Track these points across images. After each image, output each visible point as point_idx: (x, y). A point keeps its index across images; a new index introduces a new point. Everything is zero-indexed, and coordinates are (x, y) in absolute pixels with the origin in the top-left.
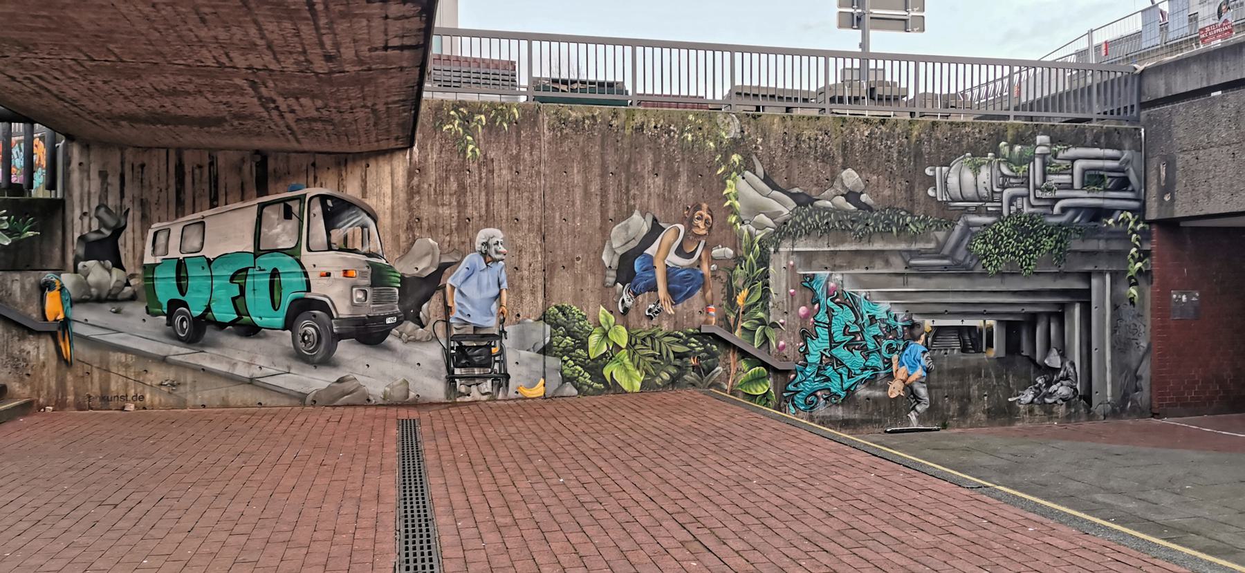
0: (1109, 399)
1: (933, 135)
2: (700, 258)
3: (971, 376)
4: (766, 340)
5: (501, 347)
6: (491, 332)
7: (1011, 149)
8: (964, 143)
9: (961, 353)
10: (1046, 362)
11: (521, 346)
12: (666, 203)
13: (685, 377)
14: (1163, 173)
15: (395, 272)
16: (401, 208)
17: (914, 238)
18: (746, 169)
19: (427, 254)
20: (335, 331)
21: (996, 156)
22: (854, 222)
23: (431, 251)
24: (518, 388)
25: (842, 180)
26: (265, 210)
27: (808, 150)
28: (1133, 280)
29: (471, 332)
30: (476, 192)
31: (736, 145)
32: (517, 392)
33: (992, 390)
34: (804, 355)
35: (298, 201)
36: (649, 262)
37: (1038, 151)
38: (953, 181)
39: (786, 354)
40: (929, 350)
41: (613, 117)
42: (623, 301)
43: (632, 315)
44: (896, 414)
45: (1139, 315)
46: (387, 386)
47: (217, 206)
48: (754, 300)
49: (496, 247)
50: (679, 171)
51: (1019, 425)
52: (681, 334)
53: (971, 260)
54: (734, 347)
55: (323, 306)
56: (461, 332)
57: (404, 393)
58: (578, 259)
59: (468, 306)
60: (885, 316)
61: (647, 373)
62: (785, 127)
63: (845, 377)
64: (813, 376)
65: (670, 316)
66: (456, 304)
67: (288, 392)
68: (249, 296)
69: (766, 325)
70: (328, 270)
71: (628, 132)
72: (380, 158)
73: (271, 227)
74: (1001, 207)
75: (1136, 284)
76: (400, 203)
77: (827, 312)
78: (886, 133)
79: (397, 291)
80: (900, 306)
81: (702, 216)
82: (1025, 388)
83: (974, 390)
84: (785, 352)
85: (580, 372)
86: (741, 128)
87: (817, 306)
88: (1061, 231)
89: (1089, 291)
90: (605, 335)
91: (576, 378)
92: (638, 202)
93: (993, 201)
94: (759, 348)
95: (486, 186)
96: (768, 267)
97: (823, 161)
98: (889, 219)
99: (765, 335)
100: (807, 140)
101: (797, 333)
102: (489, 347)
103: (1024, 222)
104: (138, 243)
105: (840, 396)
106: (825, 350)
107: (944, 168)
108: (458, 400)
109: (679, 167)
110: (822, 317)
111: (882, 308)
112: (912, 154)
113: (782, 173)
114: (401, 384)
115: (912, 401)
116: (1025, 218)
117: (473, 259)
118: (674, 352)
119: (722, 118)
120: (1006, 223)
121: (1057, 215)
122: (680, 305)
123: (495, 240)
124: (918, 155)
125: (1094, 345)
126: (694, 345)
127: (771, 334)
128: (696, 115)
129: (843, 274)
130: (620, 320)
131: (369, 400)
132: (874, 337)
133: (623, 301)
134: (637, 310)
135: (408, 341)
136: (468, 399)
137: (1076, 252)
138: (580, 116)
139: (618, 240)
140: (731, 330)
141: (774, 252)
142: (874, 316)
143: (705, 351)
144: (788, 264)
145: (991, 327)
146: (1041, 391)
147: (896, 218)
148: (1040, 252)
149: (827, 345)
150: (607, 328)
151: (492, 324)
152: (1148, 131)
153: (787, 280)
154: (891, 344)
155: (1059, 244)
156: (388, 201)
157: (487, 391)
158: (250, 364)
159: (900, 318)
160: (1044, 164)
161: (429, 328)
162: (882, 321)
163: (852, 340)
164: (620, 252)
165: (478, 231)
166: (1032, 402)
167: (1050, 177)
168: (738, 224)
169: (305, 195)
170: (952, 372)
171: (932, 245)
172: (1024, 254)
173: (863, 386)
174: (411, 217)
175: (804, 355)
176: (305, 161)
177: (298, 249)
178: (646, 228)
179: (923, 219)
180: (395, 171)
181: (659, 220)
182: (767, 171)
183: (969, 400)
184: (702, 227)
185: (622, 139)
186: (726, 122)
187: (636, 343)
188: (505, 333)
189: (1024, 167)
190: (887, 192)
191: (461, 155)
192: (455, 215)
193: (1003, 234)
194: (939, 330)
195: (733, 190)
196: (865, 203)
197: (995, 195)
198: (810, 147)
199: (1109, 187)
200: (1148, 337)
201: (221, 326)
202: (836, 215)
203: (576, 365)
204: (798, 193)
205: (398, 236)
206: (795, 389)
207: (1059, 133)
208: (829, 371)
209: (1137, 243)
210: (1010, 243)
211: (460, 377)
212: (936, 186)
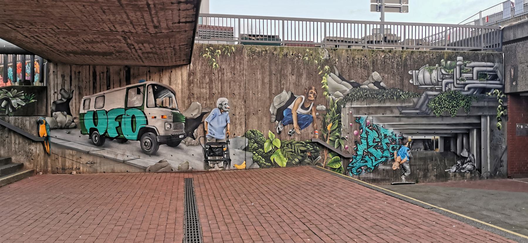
0: (489, 170)
1: (412, 57)
2: (311, 110)
3: (428, 160)
4: (340, 145)
5: (227, 148)
6: (223, 142)
7: (446, 63)
8: (426, 60)
9: (424, 151)
10: (461, 154)
11: (236, 147)
12: (297, 87)
13: (305, 160)
14: (512, 73)
15: (183, 116)
16: (185, 89)
17: (404, 101)
18: (331, 72)
19: (196, 109)
20: (158, 141)
21: (440, 66)
22: (377, 94)
23: (198, 107)
24: (234, 165)
25: (372, 76)
26: (129, 91)
27: (358, 64)
28: (499, 119)
29: (215, 141)
30: (217, 82)
31: (327, 62)
32: (234, 167)
33: (438, 167)
34: (356, 151)
35: (143, 87)
36: (290, 112)
37: (458, 63)
38: (421, 76)
39: (348, 151)
40: (410, 149)
41: (274, 50)
42: (279, 128)
43: (283, 134)
44: (396, 177)
45: (502, 134)
46: (180, 164)
47: (110, 89)
48: (335, 128)
49: (225, 105)
50: (302, 73)
51: (450, 181)
52: (303, 142)
53: (429, 110)
54: (326, 148)
55: (153, 131)
56: (210, 141)
57: (187, 167)
58: (260, 110)
59: (213, 130)
60: (391, 135)
61: (289, 159)
62: (348, 54)
63: (374, 161)
64: (360, 160)
65: (298, 135)
66: (208, 130)
67: (139, 166)
68: (123, 126)
69: (340, 138)
70: (155, 115)
71: (281, 57)
72: (177, 69)
73: (132, 98)
74: (442, 88)
75: (501, 120)
76: (185, 87)
77: (366, 133)
78: (391, 56)
79: (184, 124)
80: (397, 130)
81: (312, 92)
82: (453, 166)
83: (430, 167)
84: (348, 150)
85: (261, 158)
86: (329, 54)
87: (361, 130)
88: (468, 98)
89: (480, 124)
90: (271, 143)
91: (259, 161)
92: (285, 86)
93: (438, 85)
94: (337, 148)
95: (221, 80)
96: (341, 114)
97: (364, 68)
98: (393, 93)
99: (339, 143)
100: (357, 60)
101: (353, 142)
102: (222, 148)
103: (452, 94)
104: (77, 104)
105: (371, 169)
106: (365, 149)
107: (417, 71)
108: (209, 170)
109: (302, 71)
110: (364, 135)
111: (390, 131)
112: (403, 65)
113: (346, 73)
114: (186, 163)
115: (403, 171)
116: (452, 92)
117: (215, 111)
118: (300, 150)
119: (321, 50)
120: (444, 95)
121: (466, 91)
122: (303, 130)
123: (224, 103)
124: (405, 65)
125: (482, 147)
126: (309, 147)
127: (342, 142)
128: (310, 49)
129: (373, 117)
130: (277, 136)
131: (172, 170)
132: (386, 143)
133: (279, 128)
134: (285, 132)
135: (189, 145)
136: (213, 169)
137: (474, 107)
138: (260, 50)
139: (277, 102)
140: (325, 140)
141: (343, 107)
142: (386, 135)
143: (314, 149)
144: (349, 112)
145: (438, 139)
146: (459, 167)
147: (396, 93)
148: (459, 107)
149: (366, 147)
150: (272, 140)
151: (223, 138)
152: (506, 55)
153: (349, 119)
154: (394, 147)
155: (467, 104)
156: (180, 87)
157: (221, 166)
158: (123, 155)
159: (397, 135)
160: (461, 69)
161: (197, 140)
162: (390, 136)
163: (377, 145)
164: (277, 107)
165: (217, 99)
166: (455, 172)
167: (463, 75)
168: (328, 95)
169: (146, 84)
170: (421, 159)
171: (411, 104)
172: (452, 108)
173: (381, 165)
174: (190, 93)
175: (356, 151)
176: (145, 70)
177: (143, 107)
178: (288, 97)
179: (408, 93)
180: (183, 74)
181: (293, 93)
182: (340, 73)
183: (428, 171)
184: (312, 97)
185: (278, 60)
186: (323, 52)
187: (284, 146)
188: (229, 142)
189: (452, 70)
190: (392, 82)
191: (211, 67)
192: (208, 92)
193: (443, 99)
194: (414, 141)
195: (326, 81)
196: (382, 87)
197: (439, 82)
198: (358, 63)
199: (489, 79)
200: (506, 144)
201: (111, 139)
202: (370, 91)
203: (259, 155)
204: (353, 82)
205: (184, 101)
206: (352, 166)
207: (467, 56)
208: (367, 158)
209: (501, 103)
210: (446, 103)
211: (210, 160)
212: (413, 79)
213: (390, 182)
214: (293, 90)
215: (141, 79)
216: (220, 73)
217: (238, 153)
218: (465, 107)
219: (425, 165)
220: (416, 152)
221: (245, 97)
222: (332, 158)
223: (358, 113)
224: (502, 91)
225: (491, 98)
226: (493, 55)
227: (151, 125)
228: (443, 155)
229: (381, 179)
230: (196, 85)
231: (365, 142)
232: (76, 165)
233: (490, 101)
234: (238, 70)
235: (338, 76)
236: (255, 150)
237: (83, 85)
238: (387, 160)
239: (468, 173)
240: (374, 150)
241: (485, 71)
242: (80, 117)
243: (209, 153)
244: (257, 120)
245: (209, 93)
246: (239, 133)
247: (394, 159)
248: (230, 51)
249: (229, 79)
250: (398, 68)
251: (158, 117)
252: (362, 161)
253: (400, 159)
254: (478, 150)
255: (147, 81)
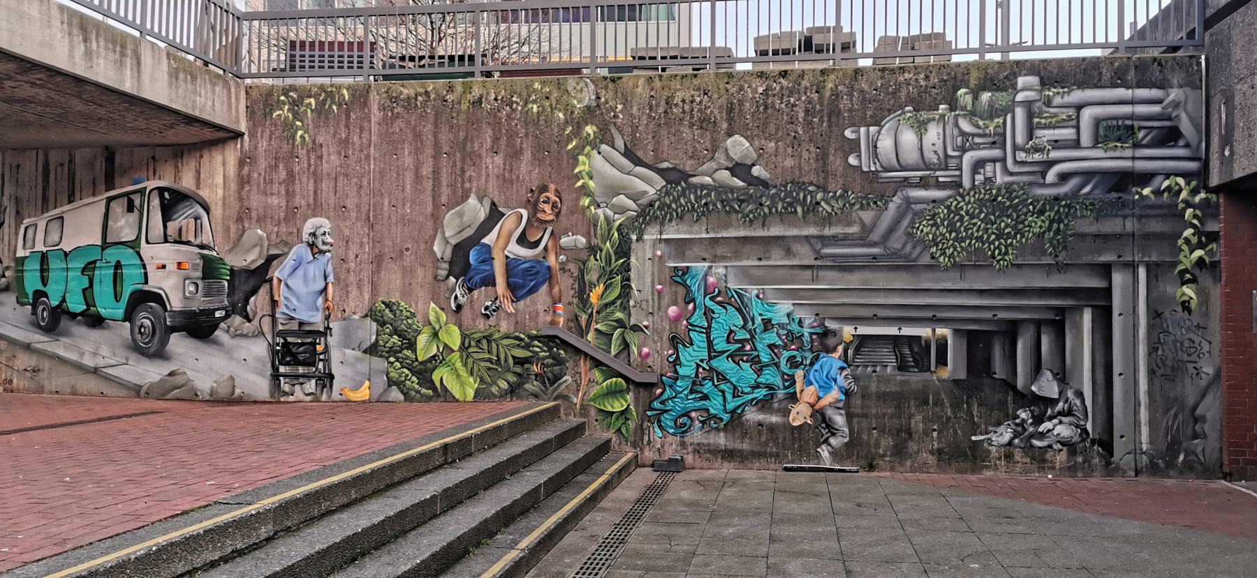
0: (1144, 447)
1: (856, 87)
2: (546, 248)
3: (912, 403)
4: (626, 346)
5: (326, 344)
6: (316, 329)
7: (976, 98)
8: (903, 94)
9: (897, 372)
10: (1033, 388)
11: (346, 345)
12: (506, 184)
13: (527, 386)
14: (1224, 116)
15: (225, 264)
16: (232, 199)
17: (828, 220)
18: (602, 142)
19: (256, 246)
20: (168, 323)
21: (952, 109)
22: (742, 201)
23: (259, 242)
24: (342, 390)
25: (726, 150)
26: (111, 204)
27: (682, 115)
28: (1188, 276)
29: (296, 328)
30: (304, 179)
31: (590, 113)
32: (341, 394)
33: (945, 424)
34: (675, 366)
35: (139, 195)
36: (486, 253)
37: (1020, 97)
38: (885, 143)
39: (651, 364)
40: (849, 366)
41: (448, 91)
42: (456, 297)
43: (466, 312)
44: (800, 446)
45: (1198, 327)
46: (215, 382)
47: (74, 201)
48: (611, 298)
49: (323, 237)
50: (521, 148)
51: (988, 474)
52: (523, 336)
53: (914, 248)
54: (586, 355)
55: (157, 298)
56: (286, 327)
57: (230, 389)
58: (407, 249)
59: (294, 300)
60: (785, 320)
61: (482, 380)
62: (652, 89)
63: (729, 396)
64: (686, 392)
65: (509, 315)
66: (282, 297)
67: (126, 383)
68: (96, 287)
69: (626, 328)
70: (163, 262)
71: (464, 107)
72: (214, 148)
73: (116, 221)
74: (961, 176)
75: (1194, 280)
76: (232, 193)
77: (705, 314)
78: (787, 88)
79: (226, 284)
80: (807, 307)
81: (548, 198)
82: (1000, 424)
83: (917, 423)
84: (649, 361)
85: (407, 375)
86: (597, 94)
87: (691, 306)
88: (1062, 208)
89: (1108, 292)
90: (435, 335)
91: (403, 382)
92: (475, 184)
93: (946, 169)
94: (616, 356)
95: (315, 173)
96: (629, 259)
97: (702, 128)
98: (792, 197)
99: (624, 339)
100: (681, 104)
101: (665, 338)
102: (314, 344)
103: (997, 196)
104: (13, 237)
105: (721, 419)
106: (702, 361)
107: (872, 129)
108: (282, 399)
109: (522, 143)
110: (699, 319)
111: (782, 309)
112: (825, 112)
113: (647, 144)
114: (227, 380)
115: (824, 432)
116: (999, 190)
117: (300, 250)
118: (514, 357)
119: (574, 84)
120: (967, 198)
121: (1052, 185)
122: (522, 302)
123: (322, 231)
124: (834, 113)
125: (1117, 368)
126: (537, 349)
127: (632, 338)
128: (543, 83)
129: (726, 267)
130: (452, 318)
131: (196, 395)
132: (769, 346)
133: (456, 297)
134: (472, 307)
135: (236, 335)
136: (291, 398)
137: (1084, 236)
138: (412, 92)
139: (453, 228)
140: (582, 333)
141: (637, 240)
142: (770, 320)
143: (552, 356)
144: (654, 255)
145: (945, 339)
146: (1025, 430)
147: (801, 195)
148: (1023, 236)
149: (705, 355)
150: (437, 327)
151: (317, 320)
152: (1211, 57)
153: (653, 274)
154: (795, 357)
155: (1055, 226)
156: (220, 192)
157: (310, 391)
158: (95, 354)
159: (807, 323)
160: (1030, 115)
161: (256, 322)
162: (782, 326)
163: (739, 350)
164: (454, 241)
165: (305, 221)
166: (1010, 443)
167: (1039, 133)
168: (592, 208)
169: (146, 188)
170: (883, 397)
171: (854, 229)
172: (997, 238)
173: (753, 409)
174: (241, 208)
175: (675, 366)
176: (144, 154)
177: (138, 241)
178: (482, 215)
179: (842, 196)
180: (227, 161)
181: (498, 204)
182: (628, 143)
183: (910, 435)
184: (549, 212)
185: (458, 115)
186: (579, 88)
187: (470, 346)
188: (331, 329)
189: (996, 120)
190: (789, 163)
191: (291, 141)
192: (284, 204)
193: (963, 213)
194: (863, 341)
195: (587, 168)
196: (757, 178)
197: (950, 161)
198: (684, 112)
199: (1145, 142)
200: (1217, 360)
201: (73, 316)
202: (718, 194)
203: (403, 367)
204: (668, 169)
205: (229, 228)
206: (662, 407)
207: (1055, 71)
208: (708, 387)
209: (1195, 222)
210: (975, 224)
211: (285, 376)
212: (860, 152)
213: (780, 462)
214: (497, 193)
215: (136, 176)
216: (313, 157)
217: (352, 360)
218: (1046, 236)
219: (900, 417)
220: (869, 377)
221: (371, 215)
222: (604, 381)
223: (681, 256)
224: (1199, 181)
225: (1153, 207)
226: (1160, 64)
227: (152, 286)
228: (963, 389)
229: (752, 451)
230: (255, 188)
231: (701, 339)
232: (6, 373)
233: (1148, 216)
234: (357, 146)
235: (623, 152)
236: (392, 352)
237: (24, 194)
238: (772, 395)
239: (1061, 450)
240: (731, 364)
241: (1131, 117)
242: (17, 265)
243: (283, 358)
244: (399, 275)
245: (287, 206)
246: (357, 306)
247: (795, 392)
248: (337, 100)
249: (334, 171)
250: (811, 122)
251: (171, 267)
252: (693, 396)
253: (815, 395)
254: (1100, 376)
255: (148, 180)
